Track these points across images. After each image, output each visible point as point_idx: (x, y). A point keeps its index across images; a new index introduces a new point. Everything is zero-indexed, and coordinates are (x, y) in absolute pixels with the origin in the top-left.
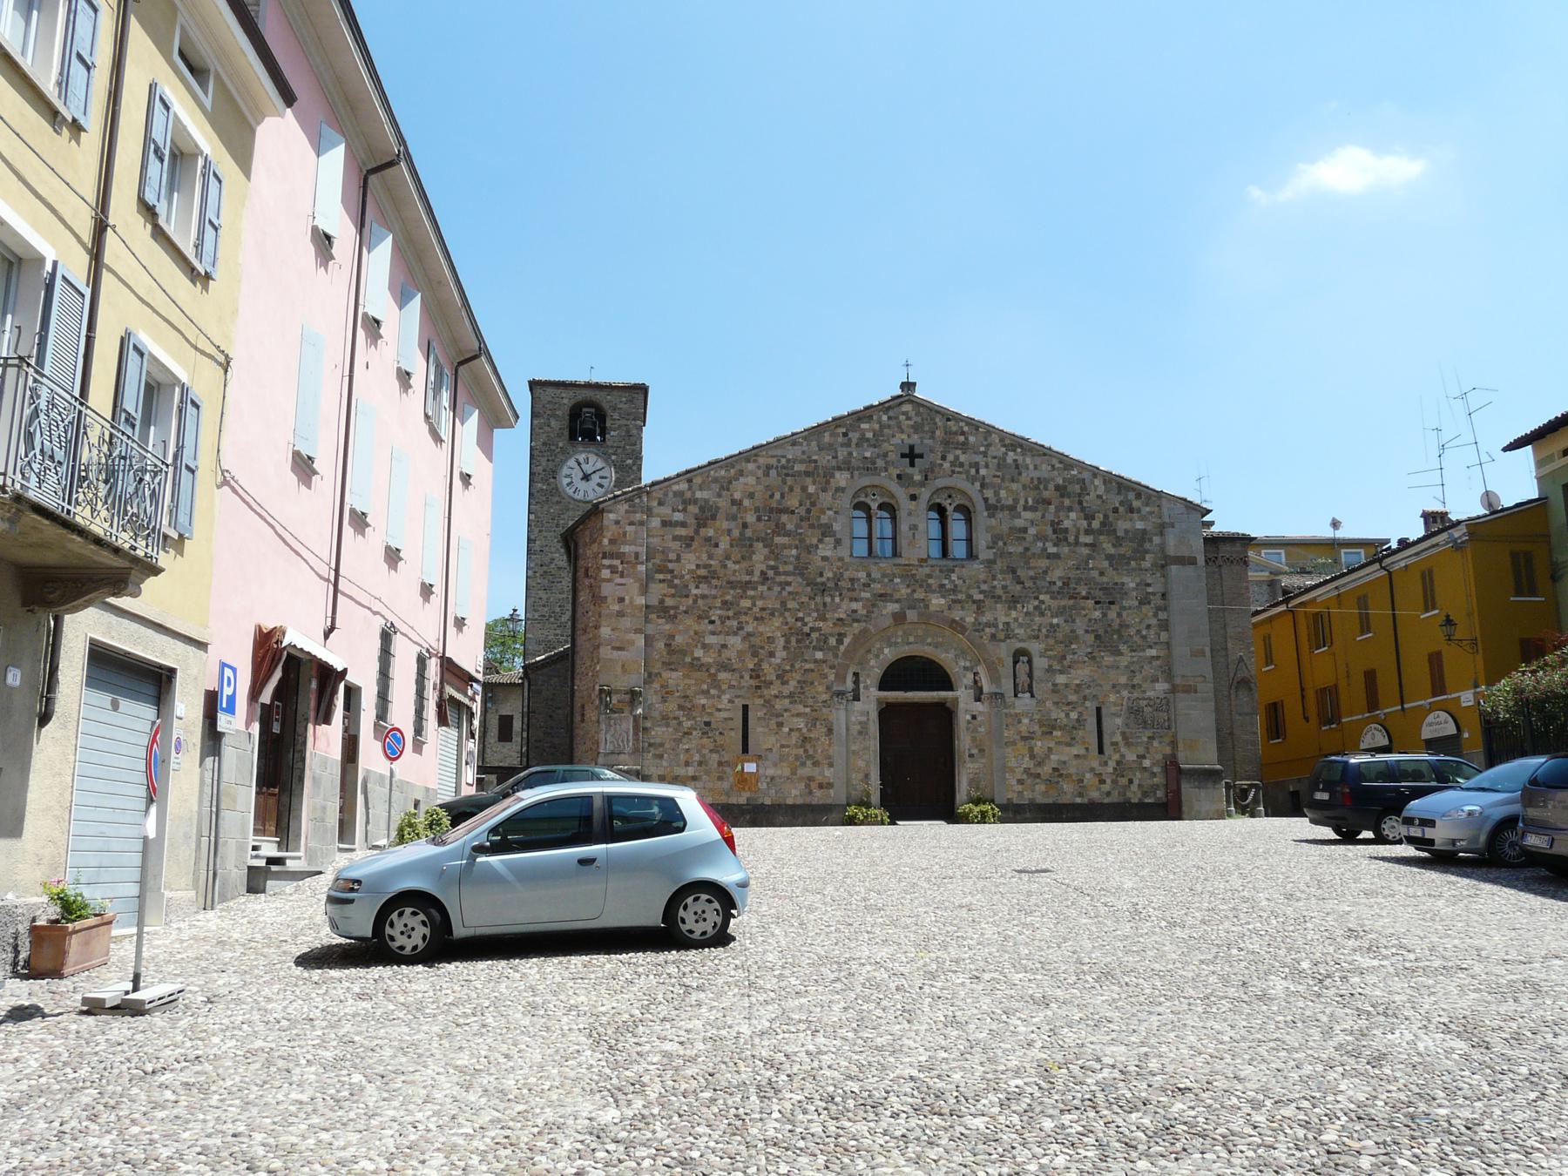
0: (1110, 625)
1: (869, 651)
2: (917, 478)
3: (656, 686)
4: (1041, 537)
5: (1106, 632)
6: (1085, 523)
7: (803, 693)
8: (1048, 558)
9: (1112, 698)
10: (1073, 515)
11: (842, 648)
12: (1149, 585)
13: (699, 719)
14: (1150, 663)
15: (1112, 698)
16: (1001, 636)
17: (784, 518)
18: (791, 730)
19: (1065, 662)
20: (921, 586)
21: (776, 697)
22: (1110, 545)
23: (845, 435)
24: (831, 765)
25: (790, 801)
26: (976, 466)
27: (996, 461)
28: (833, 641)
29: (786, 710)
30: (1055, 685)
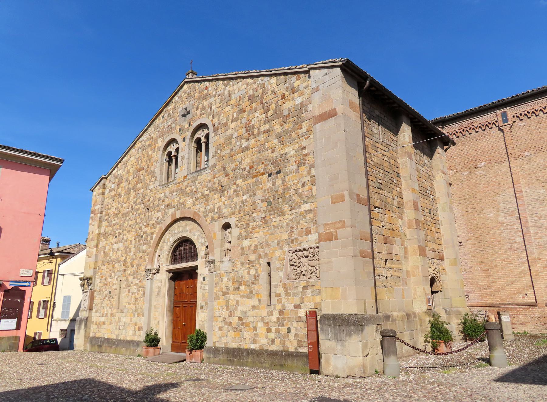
0: (277, 191)
2: (187, 126)
4: (240, 137)
5: (274, 198)
6: (264, 116)
7: (137, 272)
8: (243, 152)
9: (278, 253)
10: (257, 114)
11: (152, 241)
12: (304, 148)
13: (108, 290)
14: (304, 217)
15: (278, 253)
16: (216, 216)
17: (141, 173)
18: (132, 294)
19: (248, 229)
21: (129, 275)
22: (279, 126)
23: (163, 117)
24: (143, 315)
25: (129, 338)
26: (210, 106)
27: (220, 97)
28: (149, 238)
29: (132, 282)
30: (242, 249)
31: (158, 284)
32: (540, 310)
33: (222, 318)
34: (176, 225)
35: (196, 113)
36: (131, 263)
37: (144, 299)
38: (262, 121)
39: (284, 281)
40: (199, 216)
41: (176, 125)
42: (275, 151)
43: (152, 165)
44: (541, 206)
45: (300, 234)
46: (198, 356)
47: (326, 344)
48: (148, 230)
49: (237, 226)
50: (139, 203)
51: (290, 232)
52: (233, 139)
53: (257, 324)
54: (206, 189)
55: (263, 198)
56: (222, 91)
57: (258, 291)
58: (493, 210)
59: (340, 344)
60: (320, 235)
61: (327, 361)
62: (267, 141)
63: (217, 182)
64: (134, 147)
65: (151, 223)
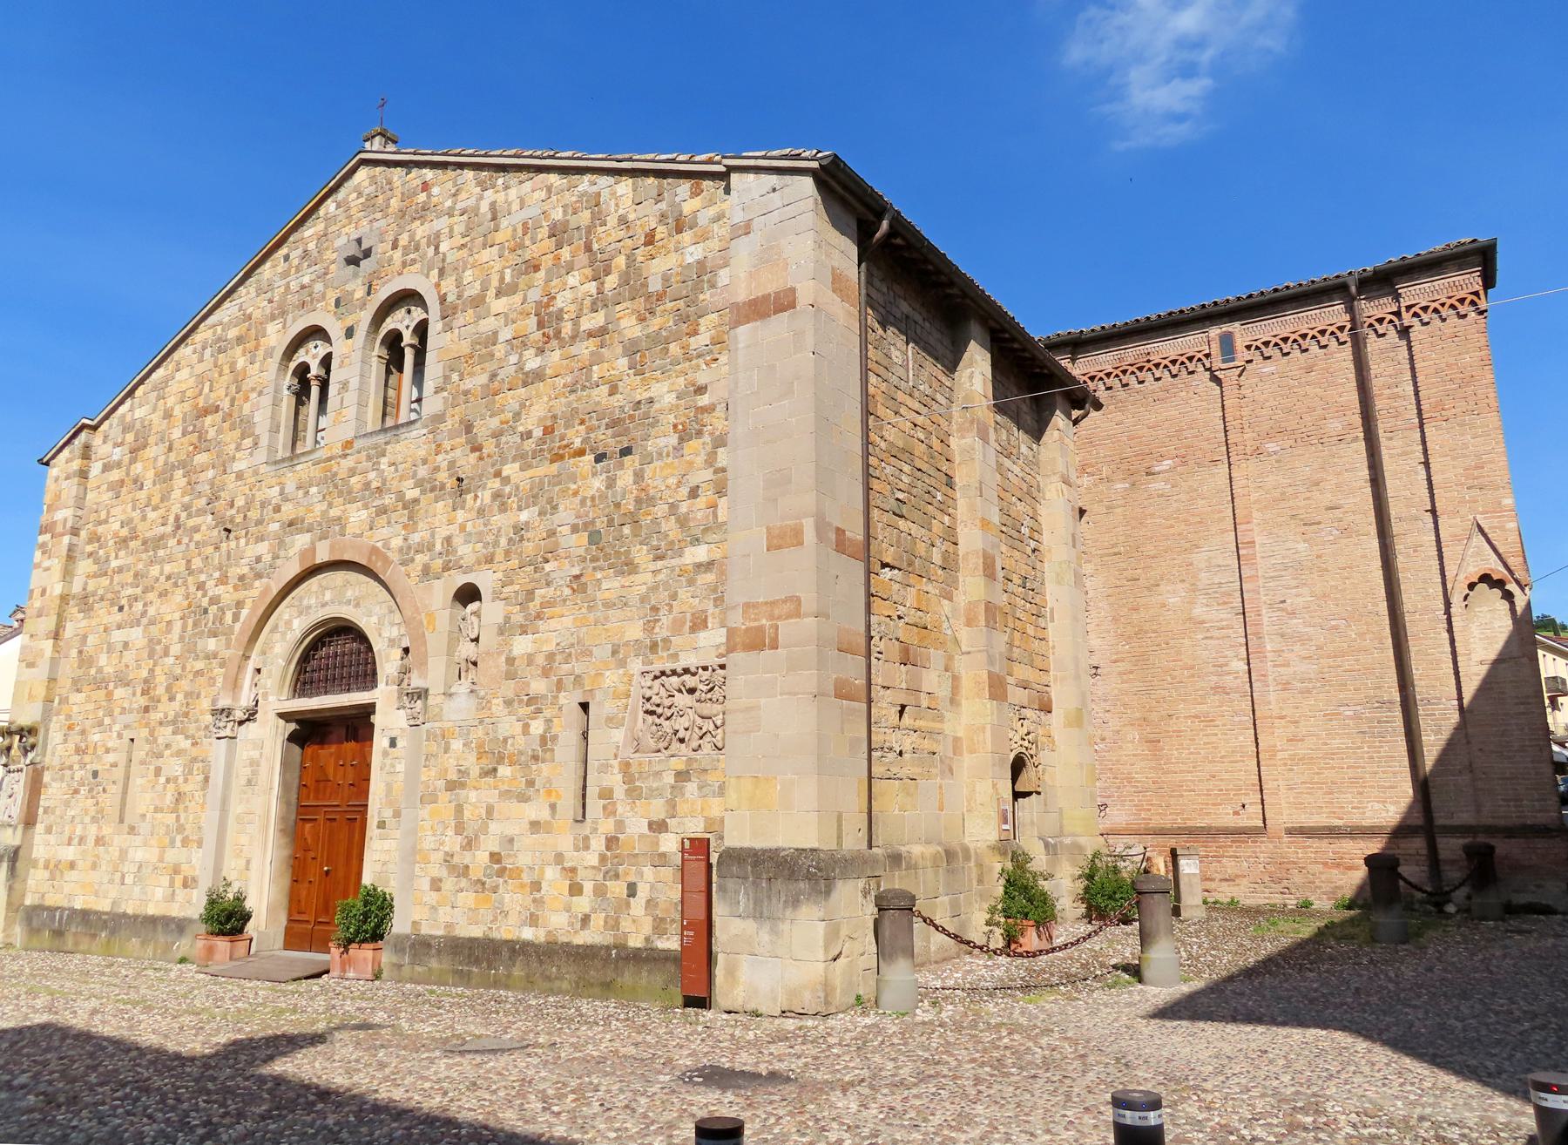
0: (617, 505)
1: (275, 629)
2: (360, 293)
3: (62, 717)
4: (519, 342)
5: (610, 523)
6: (592, 287)
7: (186, 715)
8: (525, 384)
9: (611, 678)
10: (573, 279)
11: (238, 626)
12: (701, 390)
13: (88, 767)
14: (691, 582)
15: (611, 678)
16: (438, 564)
17: (209, 420)
18: (168, 781)
20: (340, 494)
21: (161, 723)
22: (634, 319)
23: (287, 258)
24: (200, 844)
25: (151, 910)
27: (465, 217)
28: (229, 617)
29: (168, 746)
30: (511, 661)
31: (252, 753)
32: (1271, 846)
33: (441, 854)
34: (314, 583)
35: (391, 259)
36: (169, 689)
37: (204, 796)
38: (587, 302)
39: (626, 755)
40: (387, 562)
41: (326, 287)
42: (621, 390)
43: (247, 399)
44: (1294, 583)
45: (677, 627)
46: (365, 959)
47: (730, 926)
48: (227, 594)
49: (497, 596)
50: (199, 510)
51: (649, 621)
52: (498, 346)
53: (542, 872)
54: (411, 482)
55: (576, 521)
56: (472, 202)
57: (549, 781)
58: (1180, 586)
59: (767, 926)
60: (731, 633)
61: (731, 972)
62: (597, 359)
63: (444, 465)
64: (189, 340)
65: (234, 572)
